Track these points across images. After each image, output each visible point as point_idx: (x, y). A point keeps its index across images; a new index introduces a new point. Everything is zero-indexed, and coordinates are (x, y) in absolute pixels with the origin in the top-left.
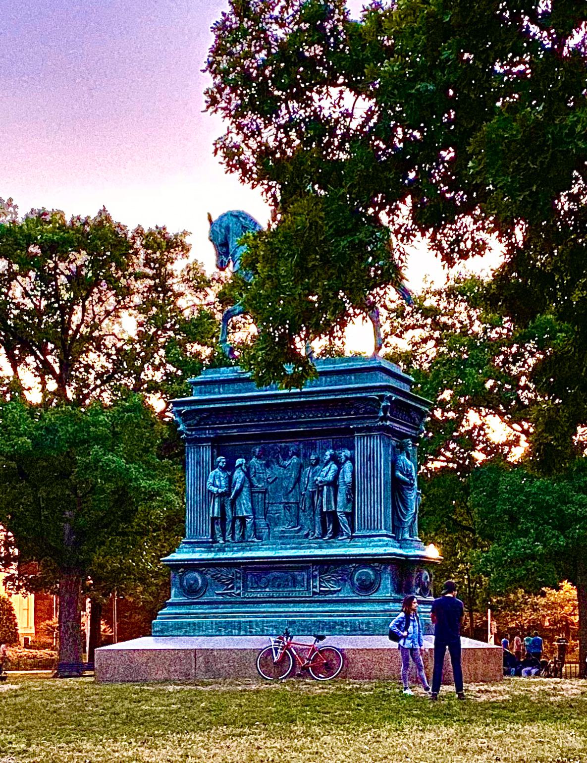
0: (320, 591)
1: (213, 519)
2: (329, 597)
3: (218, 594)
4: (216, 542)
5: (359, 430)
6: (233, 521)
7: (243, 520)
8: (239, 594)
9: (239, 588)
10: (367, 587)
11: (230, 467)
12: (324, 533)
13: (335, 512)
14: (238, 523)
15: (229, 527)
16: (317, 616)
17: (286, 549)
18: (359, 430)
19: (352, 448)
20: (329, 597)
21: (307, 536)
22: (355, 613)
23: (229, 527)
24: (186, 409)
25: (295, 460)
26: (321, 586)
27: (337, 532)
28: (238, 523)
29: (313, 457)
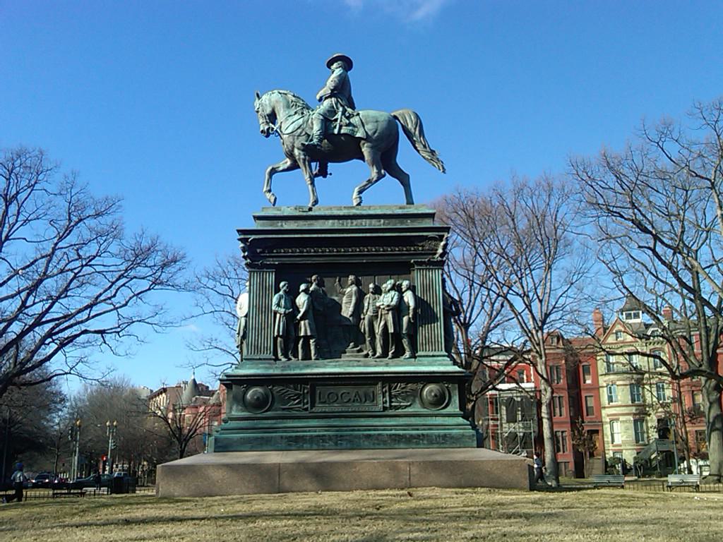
2: (400, 411)
3: (284, 409)
4: (277, 359)
8: (306, 409)
9: (307, 403)
10: (440, 401)
11: (292, 294)
12: (385, 355)
16: (391, 430)
17: (353, 366)
20: (400, 411)
21: (367, 356)
22: (431, 427)
24: (253, 237)
26: (391, 402)
27: (399, 353)
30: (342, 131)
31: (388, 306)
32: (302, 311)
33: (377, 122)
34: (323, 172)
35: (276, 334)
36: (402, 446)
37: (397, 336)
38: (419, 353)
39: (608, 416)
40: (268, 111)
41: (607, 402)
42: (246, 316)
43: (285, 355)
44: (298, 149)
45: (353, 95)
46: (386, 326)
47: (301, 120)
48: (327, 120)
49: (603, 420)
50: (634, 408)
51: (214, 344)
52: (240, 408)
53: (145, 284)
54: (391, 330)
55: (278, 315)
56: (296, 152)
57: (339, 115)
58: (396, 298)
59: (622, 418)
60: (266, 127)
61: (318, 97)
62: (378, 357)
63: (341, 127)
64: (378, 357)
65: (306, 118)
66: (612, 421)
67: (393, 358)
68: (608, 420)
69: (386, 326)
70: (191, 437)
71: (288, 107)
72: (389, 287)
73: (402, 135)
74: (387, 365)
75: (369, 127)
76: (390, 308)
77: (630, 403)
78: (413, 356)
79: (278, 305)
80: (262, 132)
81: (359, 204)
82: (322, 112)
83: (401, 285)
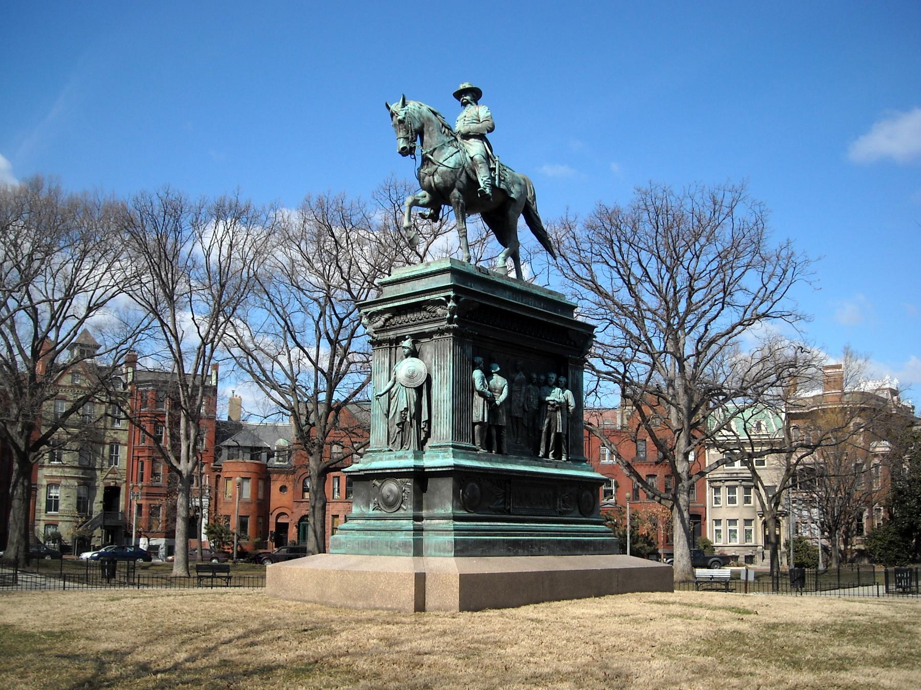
1: (474, 424)
36: (579, 552)
39: (46, 476)
40: (417, 125)
44: (459, 190)
49: (39, 482)
50: (81, 472)
66: (50, 486)
68: (44, 482)
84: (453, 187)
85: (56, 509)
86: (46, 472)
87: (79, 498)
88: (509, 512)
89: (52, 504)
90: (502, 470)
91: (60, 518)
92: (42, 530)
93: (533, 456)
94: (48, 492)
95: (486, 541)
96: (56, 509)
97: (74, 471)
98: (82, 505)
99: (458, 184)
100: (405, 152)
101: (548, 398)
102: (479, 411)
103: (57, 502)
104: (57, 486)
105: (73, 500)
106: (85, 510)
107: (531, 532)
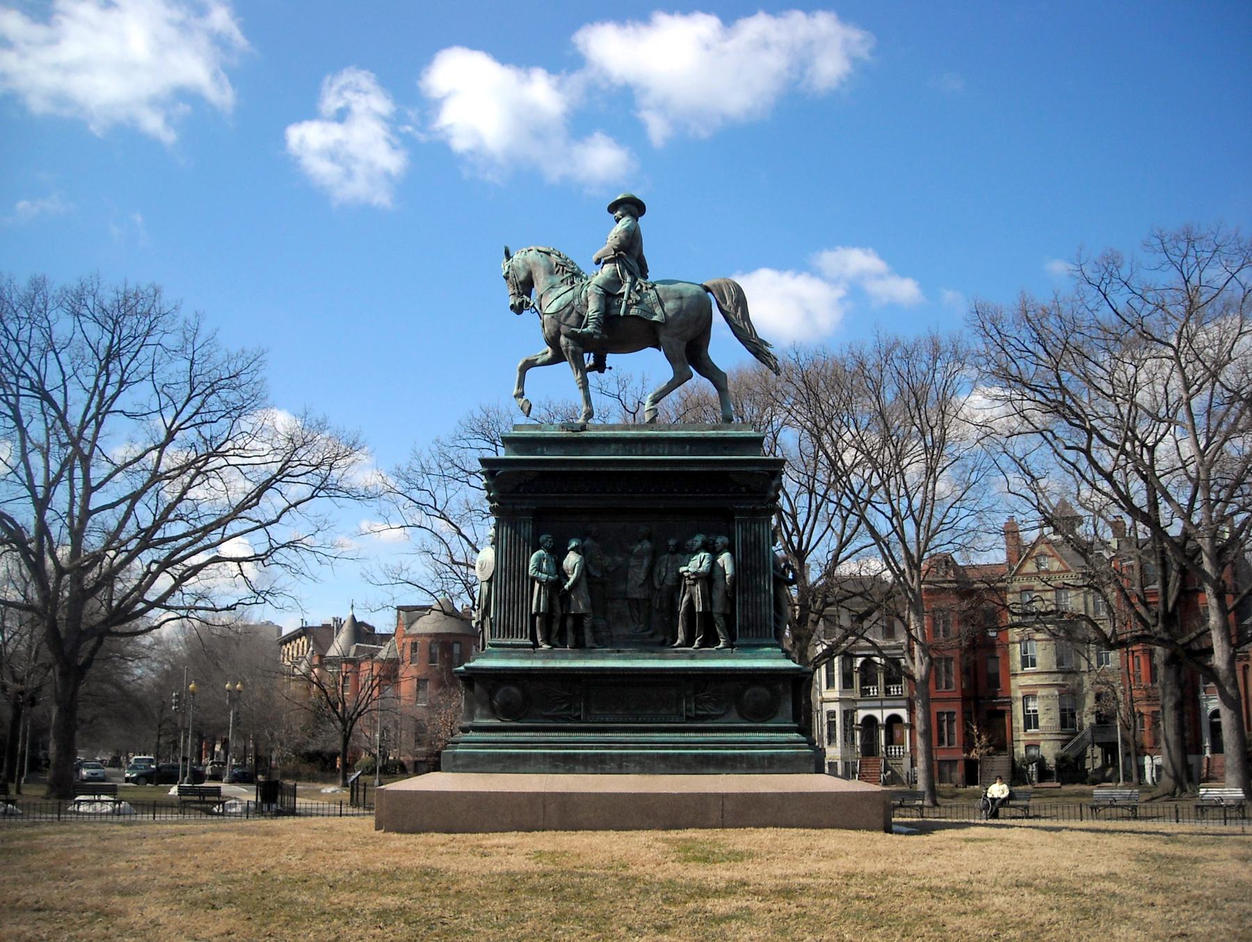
0: (697, 715)
1: (533, 617)
4: (536, 645)
5: (741, 512)
6: (564, 619)
7: (579, 618)
12: (689, 642)
13: (711, 613)
14: (570, 623)
15: (556, 627)
18: (741, 512)
19: (730, 535)
23: (556, 627)
25: (647, 545)
28: (570, 623)
29: (672, 542)
30: (633, 312)
31: (695, 573)
32: (572, 578)
33: (681, 298)
34: (600, 366)
35: (534, 610)
36: (711, 770)
37: (707, 615)
38: (739, 641)
40: (522, 276)
41: (1019, 666)
42: (490, 581)
43: (547, 640)
44: (566, 336)
45: (644, 253)
46: (691, 602)
47: (570, 294)
48: (609, 293)
49: (1013, 695)
50: (1060, 676)
51: (404, 576)
52: (485, 712)
53: (306, 491)
54: (699, 608)
55: (537, 585)
56: (563, 340)
57: (625, 289)
58: (705, 563)
59: (1041, 692)
60: (519, 300)
61: (594, 258)
62: (680, 646)
63: (628, 307)
64: (680, 646)
65: (577, 290)
66: (1026, 698)
67: (701, 646)
68: (1020, 694)
69: (691, 602)
70: (359, 715)
71: (551, 273)
72: (699, 543)
73: (717, 317)
74: (692, 658)
75: (670, 305)
76: (698, 577)
77: (1054, 668)
78: (730, 645)
79: (539, 569)
80: (512, 307)
81: (653, 420)
82: (601, 283)
83: (714, 542)
84: (558, 333)
85: (1036, 727)
86: (1022, 681)
87: (1062, 710)
88: (578, 719)
89: (1031, 721)
90: (553, 669)
91: (1041, 737)
92: (1023, 752)
93: (663, 644)
94: (1025, 706)
95: (510, 756)
96: (1036, 727)
97: (1054, 676)
98: (1067, 719)
99: (564, 329)
100: (518, 309)
101: (682, 569)
102: (538, 600)
103: (1036, 717)
104: (1034, 697)
105: (1055, 714)
106: (1073, 725)
107: (624, 744)
